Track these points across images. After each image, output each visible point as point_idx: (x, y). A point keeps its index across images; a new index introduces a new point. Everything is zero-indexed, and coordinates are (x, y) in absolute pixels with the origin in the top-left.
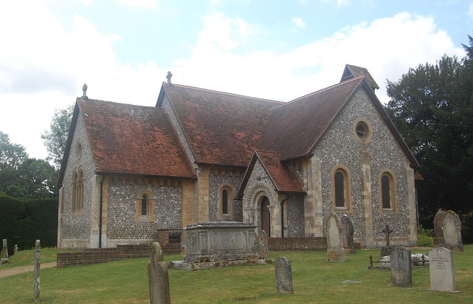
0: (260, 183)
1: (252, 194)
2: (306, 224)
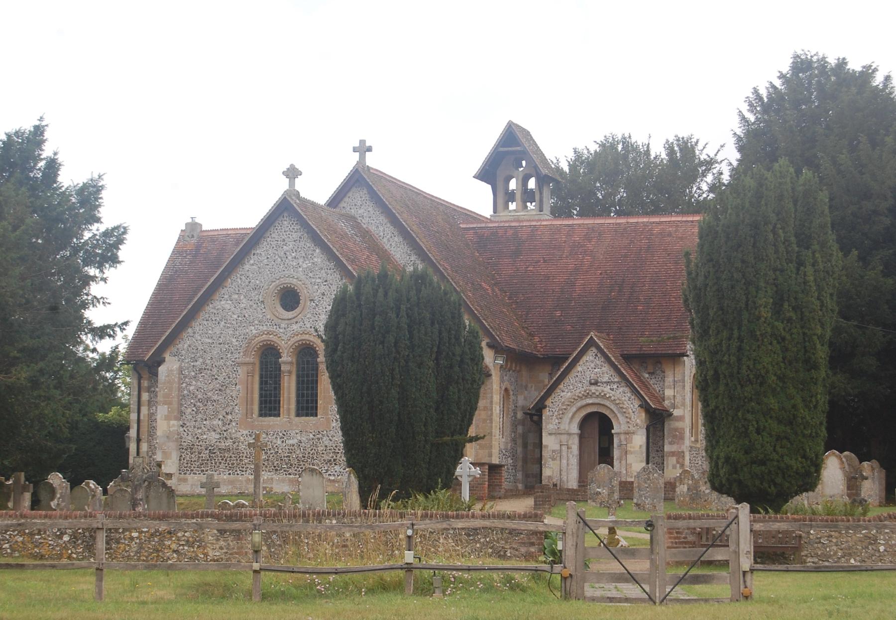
0: (597, 390)
1: (569, 407)
2: (667, 462)
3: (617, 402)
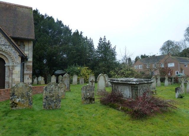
3: (8, 53)
